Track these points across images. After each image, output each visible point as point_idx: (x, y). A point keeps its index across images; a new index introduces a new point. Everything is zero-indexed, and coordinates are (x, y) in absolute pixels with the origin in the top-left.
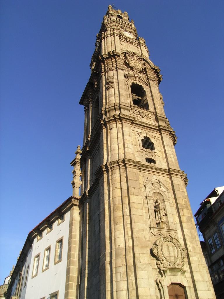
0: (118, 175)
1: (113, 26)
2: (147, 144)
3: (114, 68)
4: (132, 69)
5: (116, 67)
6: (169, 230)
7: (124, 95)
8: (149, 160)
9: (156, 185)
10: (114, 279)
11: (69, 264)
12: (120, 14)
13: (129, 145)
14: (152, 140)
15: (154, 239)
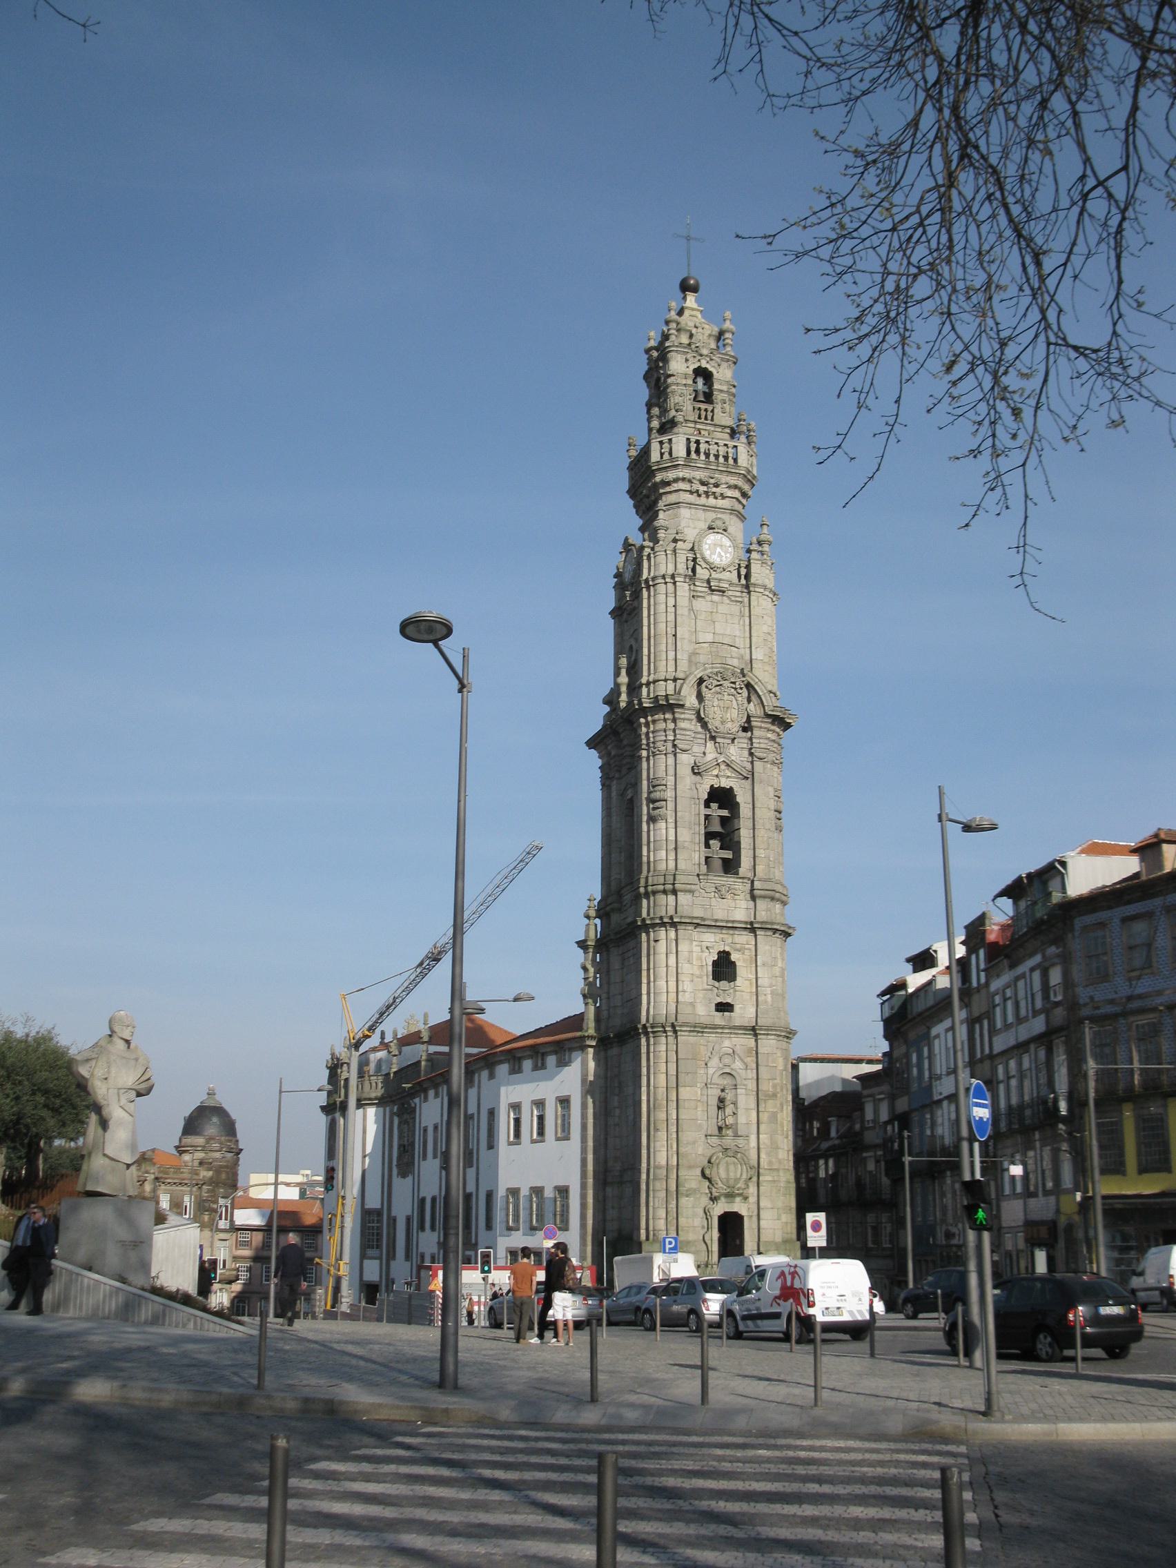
0: (663, 1048)
1: (676, 480)
2: (723, 968)
3: (670, 749)
4: (713, 738)
5: (674, 746)
6: (736, 1135)
7: (686, 844)
8: (724, 1007)
9: (727, 1060)
10: (651, 1204)
11: (584, 1150)
12: (704, 364)
13: (686, 985)
14: (733, 957)
15: (709, 1152)
